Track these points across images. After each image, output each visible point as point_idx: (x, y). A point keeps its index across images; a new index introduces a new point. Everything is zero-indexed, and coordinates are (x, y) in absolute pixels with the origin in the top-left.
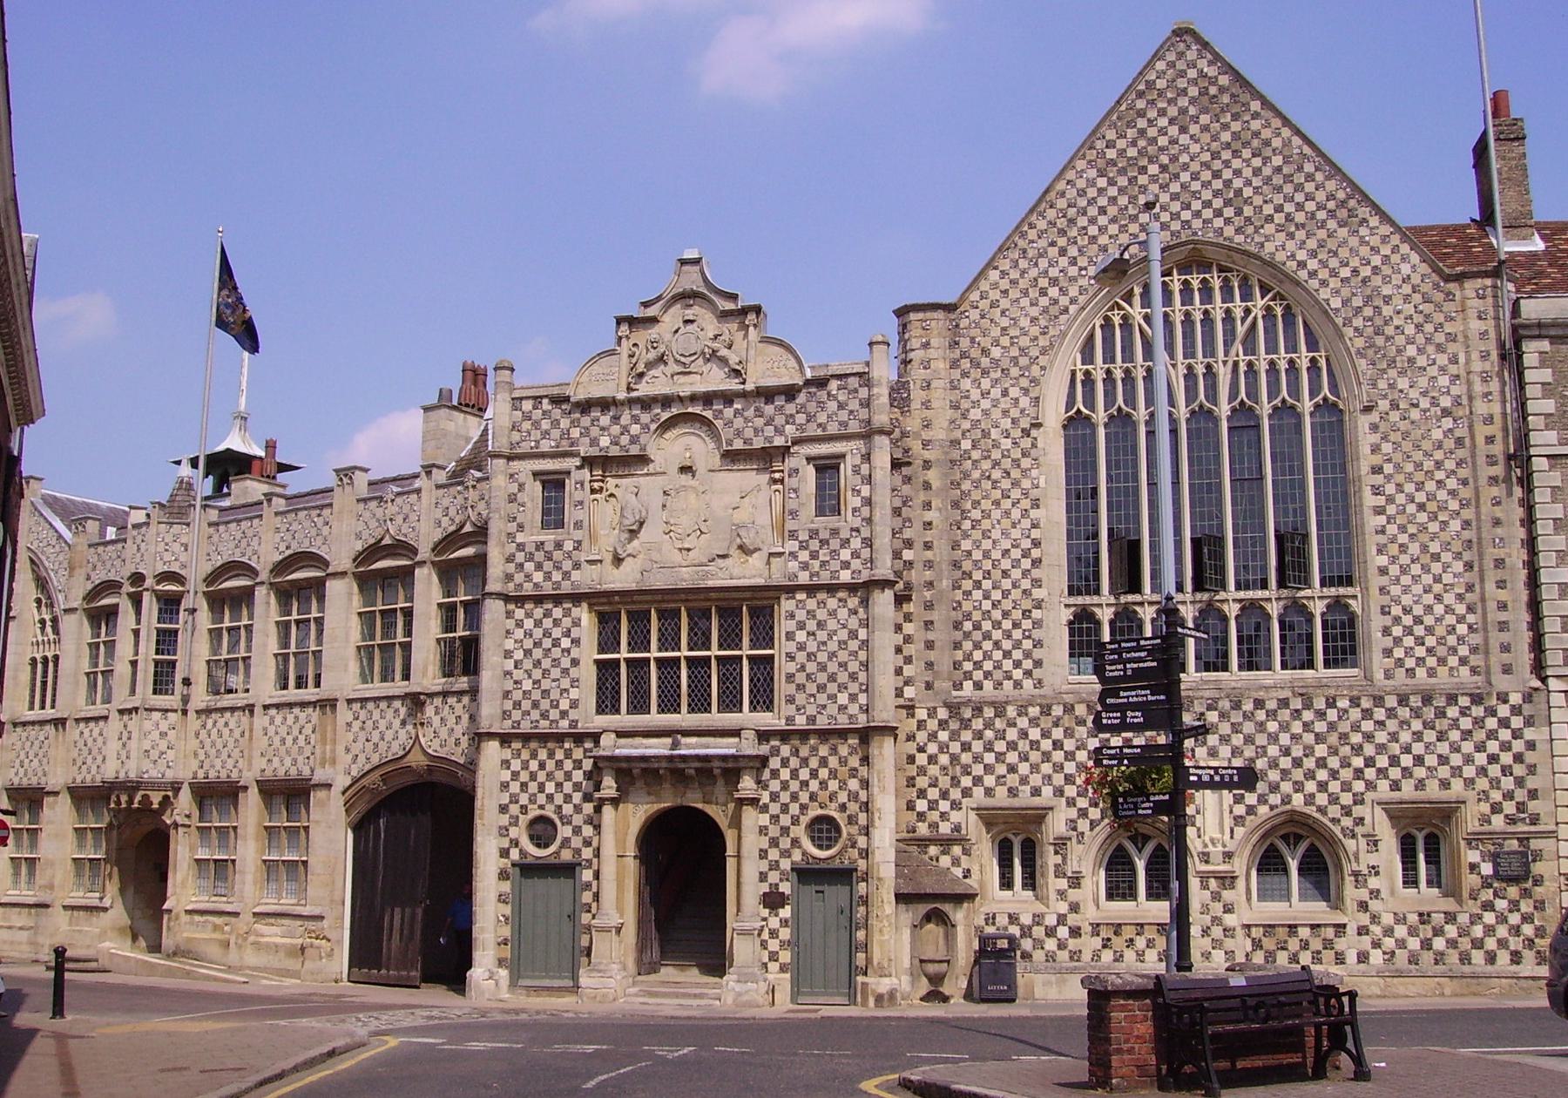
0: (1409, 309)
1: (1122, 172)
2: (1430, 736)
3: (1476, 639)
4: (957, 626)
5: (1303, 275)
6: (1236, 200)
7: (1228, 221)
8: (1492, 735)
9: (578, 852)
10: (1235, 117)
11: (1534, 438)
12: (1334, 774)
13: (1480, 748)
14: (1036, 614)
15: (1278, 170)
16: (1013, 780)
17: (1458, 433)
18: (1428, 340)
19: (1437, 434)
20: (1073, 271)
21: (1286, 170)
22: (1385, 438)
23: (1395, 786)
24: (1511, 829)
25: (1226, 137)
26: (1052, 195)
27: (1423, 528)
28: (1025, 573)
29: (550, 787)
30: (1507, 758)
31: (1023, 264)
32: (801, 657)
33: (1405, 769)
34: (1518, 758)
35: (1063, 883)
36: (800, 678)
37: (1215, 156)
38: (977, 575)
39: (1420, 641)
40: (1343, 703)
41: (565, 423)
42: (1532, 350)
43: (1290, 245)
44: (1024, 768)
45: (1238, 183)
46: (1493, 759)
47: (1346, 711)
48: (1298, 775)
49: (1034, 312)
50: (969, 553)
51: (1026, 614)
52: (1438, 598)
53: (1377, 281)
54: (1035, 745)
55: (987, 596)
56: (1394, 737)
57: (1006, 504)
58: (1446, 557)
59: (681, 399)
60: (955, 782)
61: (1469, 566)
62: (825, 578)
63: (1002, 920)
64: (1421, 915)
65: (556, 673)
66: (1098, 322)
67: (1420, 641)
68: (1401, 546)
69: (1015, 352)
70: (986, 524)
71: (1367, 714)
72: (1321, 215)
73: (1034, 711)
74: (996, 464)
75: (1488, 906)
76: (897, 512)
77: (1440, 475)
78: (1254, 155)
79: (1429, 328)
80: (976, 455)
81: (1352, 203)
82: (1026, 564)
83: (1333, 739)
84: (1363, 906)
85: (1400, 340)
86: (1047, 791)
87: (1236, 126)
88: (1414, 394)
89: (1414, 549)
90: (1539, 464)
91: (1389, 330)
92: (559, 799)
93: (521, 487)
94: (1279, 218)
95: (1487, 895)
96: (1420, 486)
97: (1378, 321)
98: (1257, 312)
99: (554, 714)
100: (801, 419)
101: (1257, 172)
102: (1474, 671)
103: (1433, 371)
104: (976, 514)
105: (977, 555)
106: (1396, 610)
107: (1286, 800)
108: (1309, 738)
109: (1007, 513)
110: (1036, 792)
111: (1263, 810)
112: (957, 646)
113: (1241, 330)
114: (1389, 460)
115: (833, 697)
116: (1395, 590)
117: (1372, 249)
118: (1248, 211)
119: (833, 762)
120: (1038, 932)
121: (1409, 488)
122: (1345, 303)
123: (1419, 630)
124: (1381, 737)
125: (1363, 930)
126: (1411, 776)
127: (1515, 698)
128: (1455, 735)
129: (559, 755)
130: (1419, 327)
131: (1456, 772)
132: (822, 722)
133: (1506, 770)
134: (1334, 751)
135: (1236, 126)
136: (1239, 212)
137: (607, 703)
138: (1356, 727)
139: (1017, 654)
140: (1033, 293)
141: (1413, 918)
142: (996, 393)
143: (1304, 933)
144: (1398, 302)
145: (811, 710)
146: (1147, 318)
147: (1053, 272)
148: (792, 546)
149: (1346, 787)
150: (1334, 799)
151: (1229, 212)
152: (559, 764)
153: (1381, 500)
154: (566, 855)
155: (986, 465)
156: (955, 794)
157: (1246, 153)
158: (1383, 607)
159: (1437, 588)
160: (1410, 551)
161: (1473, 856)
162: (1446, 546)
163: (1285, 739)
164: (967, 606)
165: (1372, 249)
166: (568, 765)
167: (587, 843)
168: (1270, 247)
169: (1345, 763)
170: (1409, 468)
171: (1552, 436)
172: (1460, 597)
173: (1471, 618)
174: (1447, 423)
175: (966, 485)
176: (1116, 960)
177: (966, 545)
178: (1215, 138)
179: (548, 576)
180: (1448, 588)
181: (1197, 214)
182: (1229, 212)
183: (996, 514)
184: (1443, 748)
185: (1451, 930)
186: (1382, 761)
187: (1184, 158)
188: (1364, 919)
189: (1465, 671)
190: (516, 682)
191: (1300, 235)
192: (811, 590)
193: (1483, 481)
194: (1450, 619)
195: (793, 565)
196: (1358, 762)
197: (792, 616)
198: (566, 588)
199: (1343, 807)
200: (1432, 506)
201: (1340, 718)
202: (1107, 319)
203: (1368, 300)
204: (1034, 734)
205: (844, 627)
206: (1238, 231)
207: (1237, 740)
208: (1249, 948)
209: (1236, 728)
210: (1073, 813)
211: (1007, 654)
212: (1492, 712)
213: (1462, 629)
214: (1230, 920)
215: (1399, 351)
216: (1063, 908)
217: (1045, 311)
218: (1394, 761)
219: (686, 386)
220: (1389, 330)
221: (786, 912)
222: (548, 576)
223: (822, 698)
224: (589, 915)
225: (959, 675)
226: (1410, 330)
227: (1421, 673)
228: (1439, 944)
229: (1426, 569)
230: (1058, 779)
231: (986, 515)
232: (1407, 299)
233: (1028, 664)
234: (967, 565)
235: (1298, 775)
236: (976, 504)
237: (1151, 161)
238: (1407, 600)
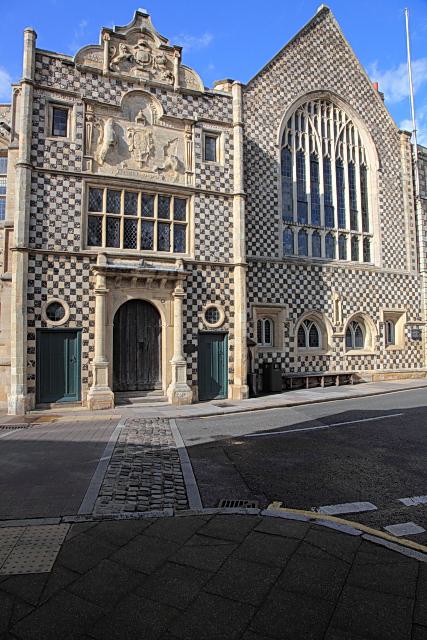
9: (80, 323)
14: (276, 225)
16: (269, 295)
19: (396, 185)
20: (289, 88)
28: (272, 208)
29: (61, 285)
32: (203, 226)
35: (287, 340)
36: (202, 237)
41: (70, 78)
44: (273, 290)
51: (272, 225)
54: (277, 280)
55: (257, 215)
59: (139, 84)
62: (213, 189)
63: (265, 356)
65: (65, 218)
70: (257, 184)
73: (277, 266)
74: (261, 159)
80: (253, 153)
82: (272, 203)
86: (282, 300)
92: (67, 292)
93: (42, 107)
94: (354, 93)
98: (344, 125)
99: (64, 242)
100: (201, 110)
104: (253, 178)
105: (253, 196)
107: (359, 309)
110: (278, 301)
111: (351, 312)
113: (339, 134)
118: (345, 87)
119: (217, 280)
129: (68, 266)
132: (212, 260)
135: (341, 53)
136: (342, 86)
137: (93, 238)
139: (269, 241)
140: (275, 92)
142: (261, 129)
143: (363, 358)
145: (207, 253)
147: (282, 86)
151: (339, 85)
152: (68, 272)
154: (72, 325)
155: (257, 158)
166: (73, 272)
167: (85, 318)
178: (335, 55)
179: (59, 162)
183: (261, 180)
187: (325, 59)
190: (38, 221)
195: (199, 181)
198: (71, 169)
205: (223, 215)
210: (291, 310)
211: (265, 241)
216: (288, 350)
219: (144, 77)
221: (195, 355)
222: (59, 162)
223: (212, 248)
224: (87, 360)
228: (397, 361)
230: (286, 296)
231: (257, 179)
233: (273, 246)
236: (253, 174)
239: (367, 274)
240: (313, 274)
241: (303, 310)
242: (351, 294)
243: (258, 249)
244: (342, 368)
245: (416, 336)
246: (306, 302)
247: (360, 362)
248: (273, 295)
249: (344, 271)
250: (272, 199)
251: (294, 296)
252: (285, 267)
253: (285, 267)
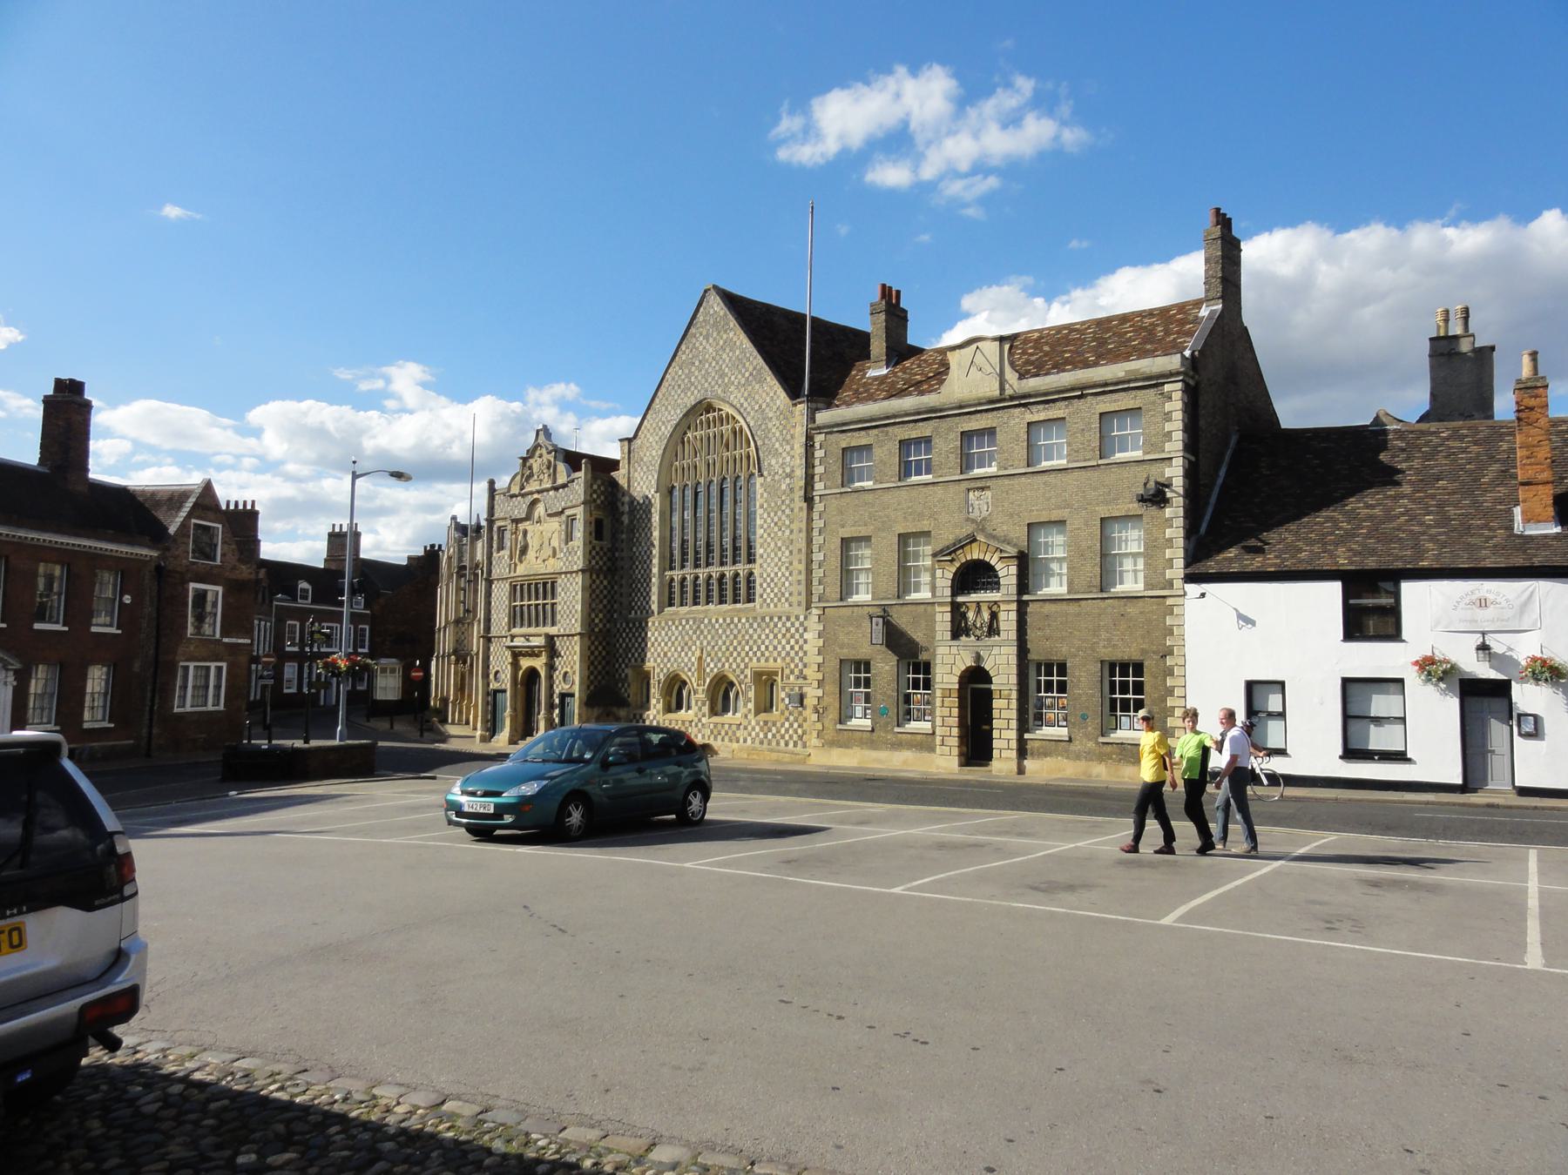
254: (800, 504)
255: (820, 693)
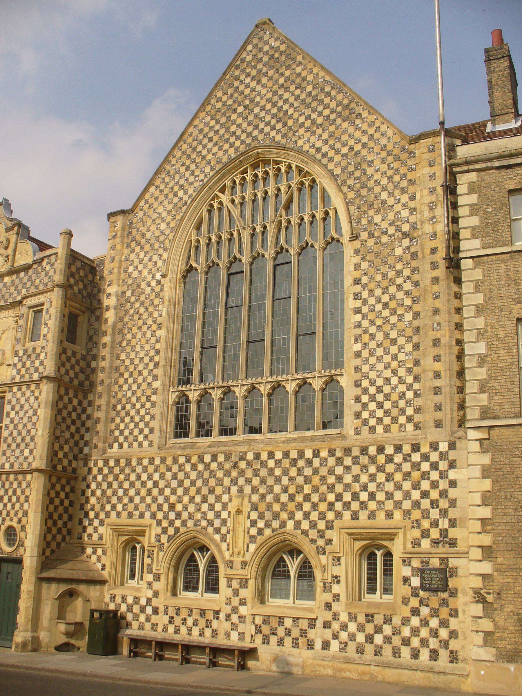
0: (384, 167)
1: (224, 114)
2: (381, 477)
3: (418, 402)
4: (114, 407)
5: (319, 156)
6: (282, 117)
7: (278, 132)
8: (425, 476)
10: (288, 68)
11: (464, 245)
12: (315, 507)
13: (416, 486)
14: (154, 398)
15: (310, 94)
17: (412, 250)
18: (396, 187)
20: (192, 179)
21: (314, 93)
22: (363, 259)
23: (355, 516)
24: (433, 550)
25: (281, 81)
26: (186, 136)
27: (386, 321)
30: (434, 494)
31: (167, 179)
33: (362, 503)
34: (444, 494)
37: (275, 93)
38: (126, 375)
39: (380, 406)
40: (324, 454)
42: (464, 182)
43: (313, 139)
44: (137, 500)
45: (286, 107)
46: (425, 494)
47: (326, 459)
48: (291, 506)
49: (170, 207)
50: (124, 361)
51: (148, 398)
52: (394, 372)
53: (364, 152)
54: (144, 484)
55: (130, 389)
56: (356, 479)
57: (144, 329)
58: (401, 341)
60: (103, 508)
61: (417, 347)
63: (118, 600)
64: (367, 615)
66: (205, 208)
67: (380, 406)
68: (371, 335)
69: (157, 233)
70: (133, 343)
71: (340, 461)
72: (333, 116)
75: (415, 612)
76: (90, 338)
77: (399, 281)
78: (297, 88)
79: (397, 178)
81: (352, 105)
83: (316, 480)
84: (328, 606)
85: (377, 189)
86: (147, 515)
87: (287, 73)
88: (384, 225)
89: (379, 336)
90: (466, 264)
91: (371, 183)
94: (308, 124)
95: (414, 602)
96: (385, 291)
97: (364, 179)
101: (297, 98)
102: (417, 427)
103: (398, 207)
105: (127, 362)
106: (365, 383)
107: (283, 525)
108: (300, 480)
109: (144, 334)
111: (268, 532)
112: (113, 420)
114: (365, 274)
115: (22, 452)
116: (365, 368)
117: (363, 132)
118: (290, 123)
120: (136, 609)
121: (378, 292)
122: (343, 170)
123: (380, 397)
124: (348, 479)
125: (327, 625)
126: (366, 508)
127: (443, 446)
128: (398, 477)
130: (390, 178)
131: (398, 505)
132: (16, 467)
133: (434, 504)
134: (316, 489)
136: (285, 125)
138: (331, 472)
141: (361, 619)
144: (377, 163)
146: (233, 201)
147: (182, 182)
148: (16, 360)
149: (322, 516)
150: (313, 525)
153: (359, 303)
156: (102, 516)
157: (292, 88)
158: (356, 382)
159: (394, 364)
160: (377, 339)
161: (407, 571)
162: (402, 332)
163: (285, 481)
164: (120, 395)
165: (363, 132)
168: (300, 143)
169: (323, 499)
170: (379, 277)
171: (476, 243)
172: (409, 371)
173: (416, 386)
174: (406, 242)
175: (126, 319)
176: (175, 633)
177: (123, 356)
180: (401, 364)
181: (261, 131)
182: (279, 126)
183: (139, 336)
184: (390, 486)
185: (387, 630)
186: (347, 497)
187: (258, 99)
188: (328, 616)
189: (410, 427)
191: (319, 131)
192: (19, 384)
193: (428, 281)
194: (402, 388)
196: (331, 497)
197: (10, 402)
199: (319, 531)
200: (393, 304)
201: (321, 465)
202: (211, 206)
203: (357, 166)
204: (144, 477)
206: (284, 136)
207: (256, 481)
208: (253, 632)
209: (256, 473)
210: (159, 530)
212: (425, 457)
213: (410, 395)
214: (243, 610)
215: (376, 197)
217: (176, 205)
218: (355, 496)
220: (371, 183)
225: (111, 439)
226: (384, 181)
227: (380, 429)
228: (378, 639)
229: (387, 351)
231: (134, 336)
232: (383, 161)
234: (122, 369)
235: (291, 506)
237: (239, 105)
238: (372, 375)
239: (309, 454)
240: (201, 467)
241: (177, 530)
242: (269, 498)
243: (126, 438)
244: (242, 635)
245: (436, 582)
246: (185, 515)
247: (281, 632)
248: (136, 508)
249: (257, 456)
250: (152, 359)
251: (166, 507)
252: (157, 462)
253: (157, 462)
254: (431, 271)
255: (487, 568)
